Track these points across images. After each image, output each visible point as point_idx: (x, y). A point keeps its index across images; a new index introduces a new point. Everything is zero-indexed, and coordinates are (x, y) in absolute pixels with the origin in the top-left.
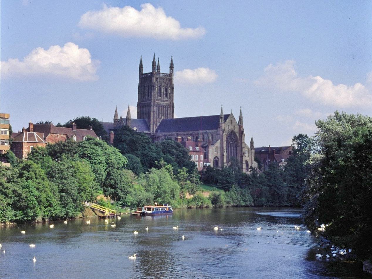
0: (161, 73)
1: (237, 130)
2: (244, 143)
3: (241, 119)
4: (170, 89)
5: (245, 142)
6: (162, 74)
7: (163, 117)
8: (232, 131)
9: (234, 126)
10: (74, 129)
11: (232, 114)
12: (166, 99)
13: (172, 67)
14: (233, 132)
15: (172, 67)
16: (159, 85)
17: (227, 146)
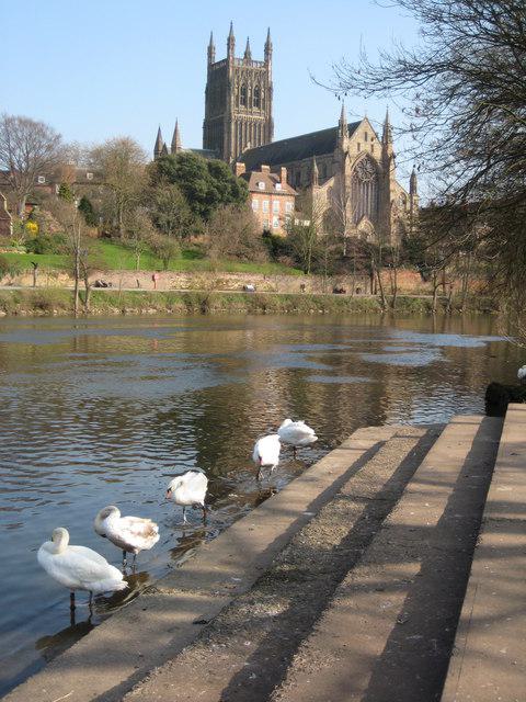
1: (377, 155)
2: (394, 180)
7: (249, 144)
12: (255, 109)
14: (370, 159)
16: (241, 83)
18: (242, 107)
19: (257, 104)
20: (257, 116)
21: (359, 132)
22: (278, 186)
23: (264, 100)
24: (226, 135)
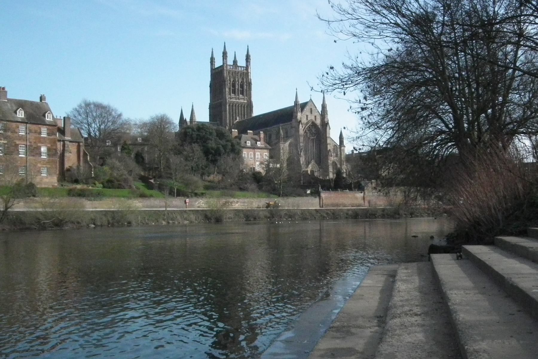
0: (238, 66)
1: (318, 122)
3: (324, 107)
4: (246, 85)
5: (331, 136)
7: (238, 118)
9: (315, 117)
11: (311, 100)
12: (241, 96)
14: (314, 124)
16: (232, 80)
18: (233, 95)
19: (242, 93)
20: (242, 100)
21: (307, 109)
22: (258, 143)
23: (246, 90)
24: (223, 113)
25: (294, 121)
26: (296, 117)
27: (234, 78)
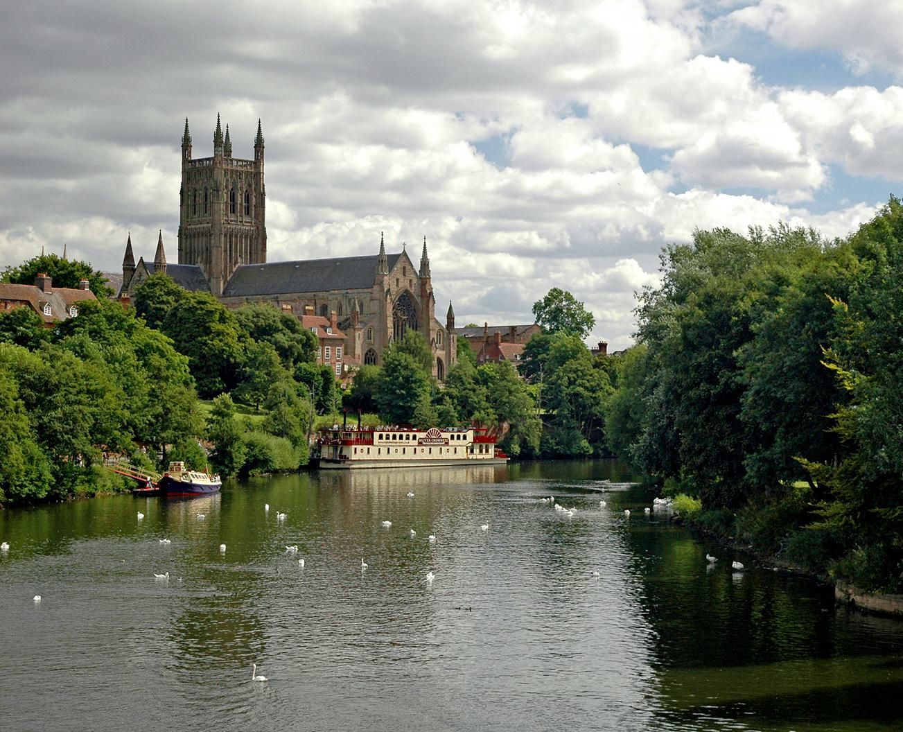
6: (238, 161)
8: (406, 291)
10: (45, 288)
12: (247, 219)
13: (259, 145)
15: (259, 145)
16: (230, 187)
17: (394, 325)
19: (248, 213)
25: (376, 288)
26: (381, 283)
27: (234, 183)
